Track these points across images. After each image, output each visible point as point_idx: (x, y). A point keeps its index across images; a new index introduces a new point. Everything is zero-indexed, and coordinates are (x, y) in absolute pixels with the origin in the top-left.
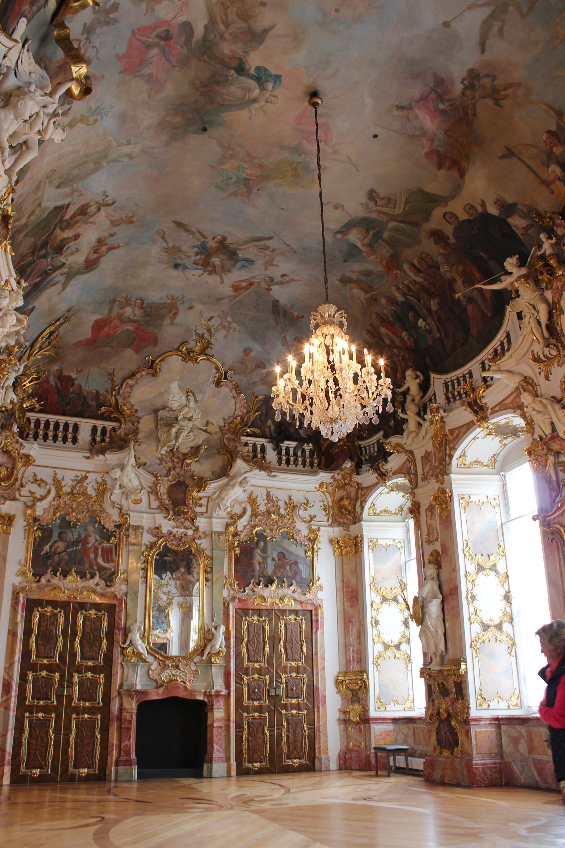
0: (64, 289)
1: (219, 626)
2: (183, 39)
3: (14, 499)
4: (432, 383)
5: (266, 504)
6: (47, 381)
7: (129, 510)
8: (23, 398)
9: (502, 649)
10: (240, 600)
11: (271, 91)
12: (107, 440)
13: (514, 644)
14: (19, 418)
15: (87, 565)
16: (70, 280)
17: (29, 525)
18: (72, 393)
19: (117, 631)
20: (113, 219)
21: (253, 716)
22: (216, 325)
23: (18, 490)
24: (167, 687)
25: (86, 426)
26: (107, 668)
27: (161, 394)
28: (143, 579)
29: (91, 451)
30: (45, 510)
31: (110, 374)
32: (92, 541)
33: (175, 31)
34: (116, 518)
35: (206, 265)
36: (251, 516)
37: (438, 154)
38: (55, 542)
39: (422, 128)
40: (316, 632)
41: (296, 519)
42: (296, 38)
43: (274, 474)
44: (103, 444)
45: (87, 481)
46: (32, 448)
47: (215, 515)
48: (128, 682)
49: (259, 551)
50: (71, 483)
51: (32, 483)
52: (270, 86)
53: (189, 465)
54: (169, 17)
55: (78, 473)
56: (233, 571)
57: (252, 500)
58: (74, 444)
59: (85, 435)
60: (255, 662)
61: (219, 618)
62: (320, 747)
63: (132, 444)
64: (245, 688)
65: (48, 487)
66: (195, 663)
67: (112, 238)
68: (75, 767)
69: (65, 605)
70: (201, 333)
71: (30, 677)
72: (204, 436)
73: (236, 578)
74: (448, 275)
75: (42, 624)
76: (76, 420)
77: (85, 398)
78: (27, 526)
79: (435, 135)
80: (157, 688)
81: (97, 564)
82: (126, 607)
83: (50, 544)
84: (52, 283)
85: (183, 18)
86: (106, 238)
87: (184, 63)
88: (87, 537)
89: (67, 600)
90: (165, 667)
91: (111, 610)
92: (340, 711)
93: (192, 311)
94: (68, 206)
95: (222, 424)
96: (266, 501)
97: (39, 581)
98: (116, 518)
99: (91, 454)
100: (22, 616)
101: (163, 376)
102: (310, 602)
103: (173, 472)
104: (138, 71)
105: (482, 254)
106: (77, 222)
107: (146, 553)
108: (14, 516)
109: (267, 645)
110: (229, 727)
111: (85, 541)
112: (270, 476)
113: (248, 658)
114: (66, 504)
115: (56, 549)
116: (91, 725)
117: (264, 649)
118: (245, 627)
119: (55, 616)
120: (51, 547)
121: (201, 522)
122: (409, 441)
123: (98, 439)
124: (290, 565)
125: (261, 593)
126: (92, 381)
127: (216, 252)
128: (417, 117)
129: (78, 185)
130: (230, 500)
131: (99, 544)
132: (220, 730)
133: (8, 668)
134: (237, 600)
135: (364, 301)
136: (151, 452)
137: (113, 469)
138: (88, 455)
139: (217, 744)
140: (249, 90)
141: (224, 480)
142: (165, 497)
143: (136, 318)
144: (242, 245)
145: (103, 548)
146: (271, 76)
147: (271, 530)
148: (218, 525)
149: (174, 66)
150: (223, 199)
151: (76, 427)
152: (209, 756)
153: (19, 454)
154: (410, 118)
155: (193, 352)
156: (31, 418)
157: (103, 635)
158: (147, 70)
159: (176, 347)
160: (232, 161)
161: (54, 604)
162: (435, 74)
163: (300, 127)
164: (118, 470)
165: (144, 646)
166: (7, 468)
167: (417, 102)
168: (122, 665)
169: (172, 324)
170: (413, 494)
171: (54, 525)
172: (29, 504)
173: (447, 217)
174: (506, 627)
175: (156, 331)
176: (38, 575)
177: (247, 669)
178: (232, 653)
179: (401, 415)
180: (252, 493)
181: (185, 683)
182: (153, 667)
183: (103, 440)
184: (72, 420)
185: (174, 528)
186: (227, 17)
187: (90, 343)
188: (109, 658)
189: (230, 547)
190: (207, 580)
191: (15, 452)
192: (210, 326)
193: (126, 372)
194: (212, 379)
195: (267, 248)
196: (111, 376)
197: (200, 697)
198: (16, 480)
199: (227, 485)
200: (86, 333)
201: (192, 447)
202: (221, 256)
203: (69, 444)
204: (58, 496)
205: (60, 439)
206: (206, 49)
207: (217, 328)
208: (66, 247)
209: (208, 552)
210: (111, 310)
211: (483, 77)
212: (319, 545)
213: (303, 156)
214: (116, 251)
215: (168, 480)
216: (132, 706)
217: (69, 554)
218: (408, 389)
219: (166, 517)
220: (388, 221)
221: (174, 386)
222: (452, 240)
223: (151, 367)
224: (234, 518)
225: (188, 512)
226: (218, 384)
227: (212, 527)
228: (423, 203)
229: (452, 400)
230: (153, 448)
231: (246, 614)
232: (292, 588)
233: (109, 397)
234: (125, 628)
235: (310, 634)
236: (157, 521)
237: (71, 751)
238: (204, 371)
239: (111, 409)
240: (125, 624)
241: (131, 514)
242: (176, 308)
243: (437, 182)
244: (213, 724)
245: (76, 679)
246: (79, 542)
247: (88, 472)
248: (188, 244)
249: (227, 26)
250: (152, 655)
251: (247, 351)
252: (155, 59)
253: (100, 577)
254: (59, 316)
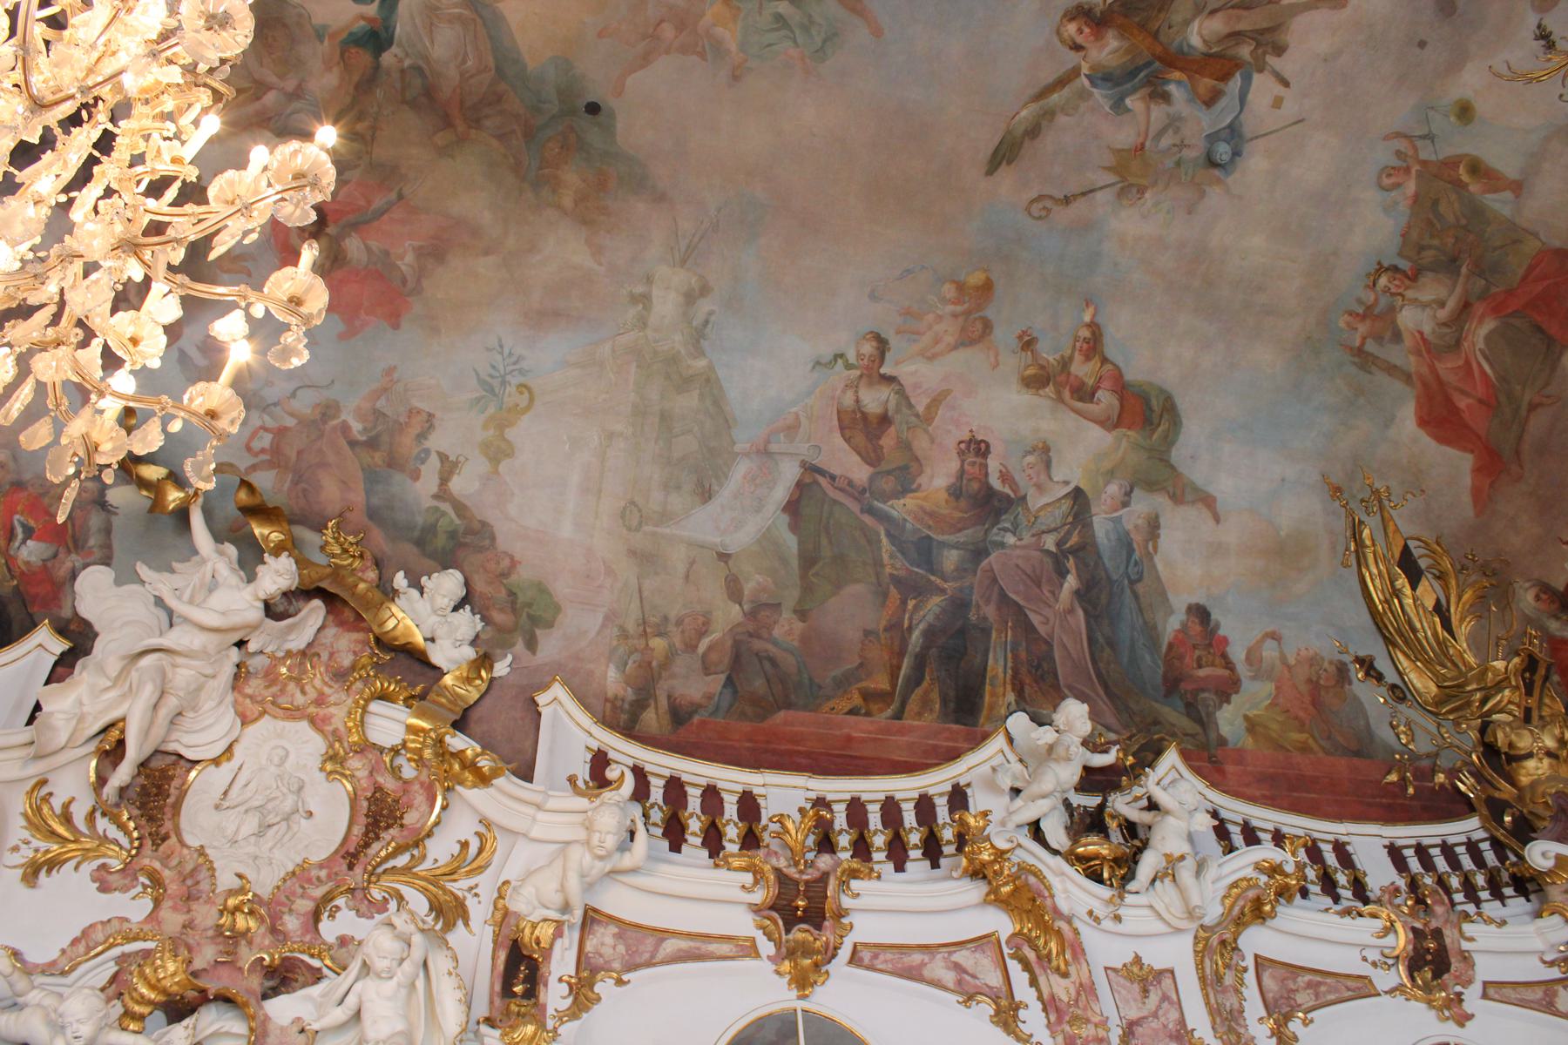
0: (1208, 501)
20: (949, 339)
84: (1137, 538)
104: (404, 282)
106: (905, 446)
127: (1155, 35)
149: (401, 197)
150: (877, 32)
160: (708, 18)
175: (1531, 247)
208: (995, 482)
210: (1391, 369)
252: (374, 244)
254: (1341, 525)
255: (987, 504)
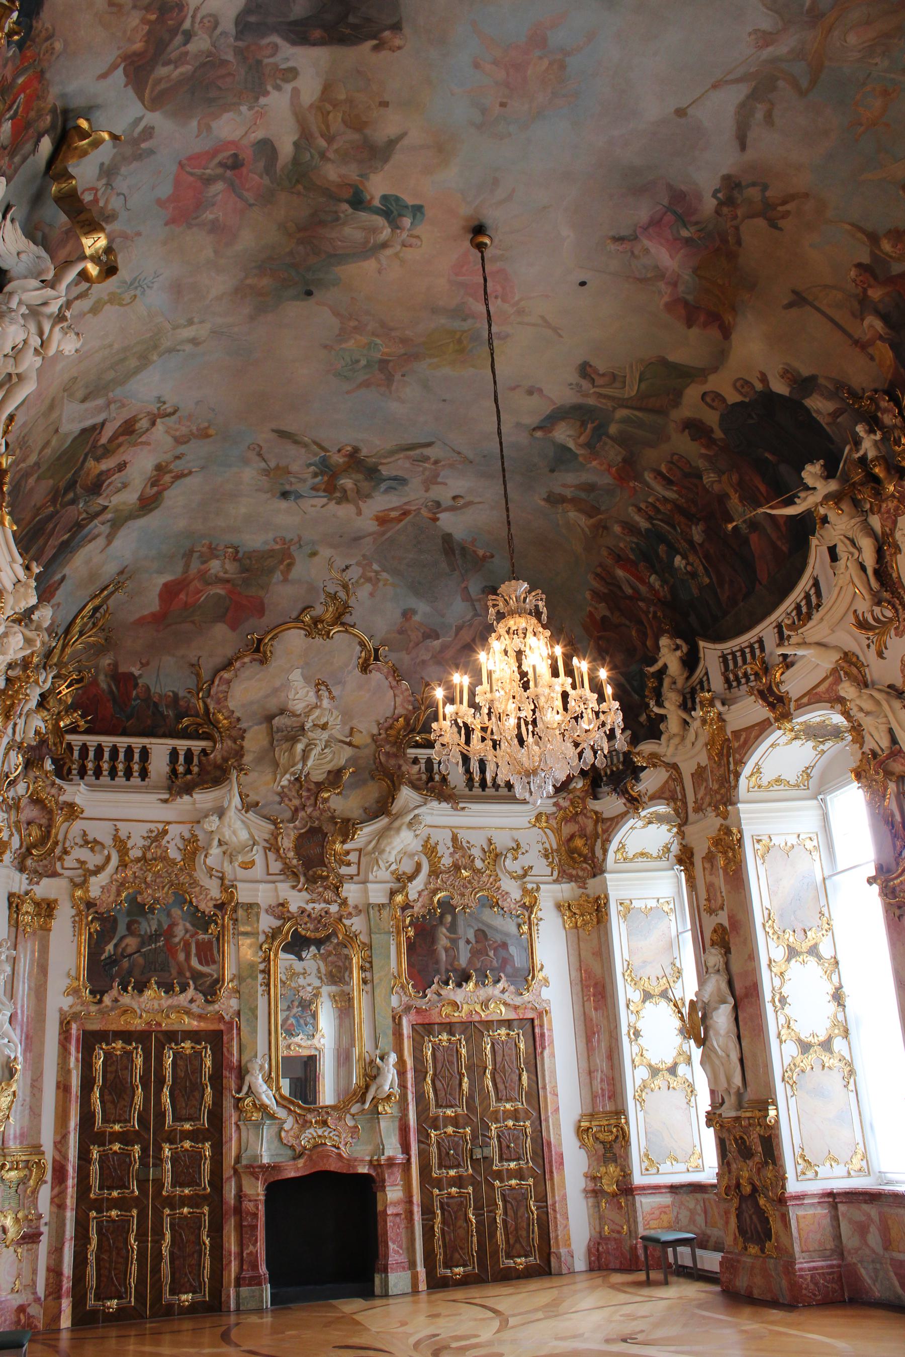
1: (388, 1054)
2: (261, 164)
3: (55, 874)
4: (701, 655)
5: (452, 855)
6: (95, 682)
7: (236, 880)
8: (59, 713)
9: (834, 1081)
10: (419, 1011)
11: (409, 230)
12: (195, 769)
13: (852, 1072)
14: (55, 744)
15: (174, 972)
16: (119, 528)
17: (79, 913)
18: (135, 700)
19: (227, 1073)
20: (178, 434)
21: (449, 1194)
22: (356, 576)
23: (60, 859)
24: (310, 1156)
25: (160, 750)
26: (215, 1133)
27: (276, 691)
28: (264, 988)
29: (170, 789)
30: (103, 887)
31: (193, 665)
32: (179, 931)
33: (247, 154)
34: (215, 892)
35: (331, 489)
36: (430, 876)
37: (686, 303)
38: (122, 938)
39: (657, 267)
40: (542, 1053)
41: (501, 875)
42: (442, 148)
43: (461, 805)
44: (189, 777)
45: (167, 838)
46: (78, 793)
47: (371, 878)
48: (249, 1152)
49: (444, 930)
50: (141, 843)
51: (81, 846)
52: (407, 222)
53: (326, 800)
54: (236, 135)
55: (152, 826)
56: (404, 965)
57: (430, 850)
58: (143, 780)
59: (159, 764)
60: (447, 1107)
61: (387, 1041)
62: (557, 1236)
63: (234, 773)
64: (434, 1150)
65: (106, 852)
66: (353, 1115)
67: (178, 462)
68: (173, 1292)
69: (142, 1037)
70: (332, 592)
71: (95, 1155)
72: (348, 752)
73: (411, 976)
74: (716, 487)
75: (109, 1069)
76: (145, 741)
77: (156, 705)
78: (77, 915)
79: (679, 275)
80: (294, 1159)
81: (191, 968)
82: (239, 1034)
83: (114, 941)
84: (89, 537)
85: (259, 135)
86: (168, 464)
87: (267, 198)
88: (172, 926)
89: (147, 1028)
90: (305, 1125)
91: (216, 1039)
92: (586, 1176)
93: (316, 559)
94: (103, 424)
95: (375, 731)
96: (452, 850)
97: (100, 1001)
98: (215, 892)
99: (171, 794)
100: (77, 1060)
101: (275, 664)
102: (530, 1005)
103: (301, 814)
105: (767, 455)
106: (120, 445)
107: (265, 946)
108: (56, 901)
109: (466, 1079)
110: (410, 1213)
111: (169, 933)
112: (456, 809)
113: (437, 1101)
114: (136, 877)
115: (124, 949)
116: (195, 1224)
117: (460, 1085)
118: (429, 1053)
119: (128, 1055)
120: (116, 946)
121: (350, 891)
122: (671, 749)
123: (181, 769)
124: (495, 950)
125: (452, 996)
126: (165, 678)
127: (345, 471)
128: (647, 251)
129: (118, 393)
130: (394, 853)
131: (192, 936)
132: (398, 1219)
133: (60, 1142)
134: (413, 1011)
135: (586, 529)
136: (264, 784)
137: (206, 816)
138: (166, 796)
139: (394, 1243)
140: (375, 230)
141: (383, 821)
142: (291, 854)
143: (227, 576)
144: (386, 457)
145: (197, 943)
146: (407, 207)
147: (462, 895)
148: (377, 894)
149: (251, 205)
150: (348, 392)
151: (145, 753)
152: (381, 1262)
153: (57, 803)
154: (636, 252)
155: (322, 622)
156: (73, 743)
157: (206, 1080)
158: (209, 216)
159: (293, 616)
160: (358, 337)
161: (126, 1036)
162: (670, 187)
163: (461, 278)
164: (215, 818)
165: (271, 1093)
166: (40, 826)
167: (645, 229)
168: (238, 1126)
169: (285, 580)
170: (681, 834)
171: (119, 910)
172: (78, 880)
173: (708, 399)
174: (839, 1044)
175: (261, 593)
176: (98, 992)
177: (436, 1118)
178: (410, 1097)
179: (656, 710)
180: (429, 838)
181: (338, 1148)
182: (287, 1127)
183: (188, 771)
184: (137, 742)
185: (307, 902)
186: (328, 127)
187: (159, 619)
188: (216, 1116)
189: (397, 927)
190: (365, 982)
191: (50, 801)
192: (347, 579)
193: (218, 660)
194: (354, 661)
195: (426, 459)
196: (195, 667)
197: (363, 1170)
198: (56, 843)
199: (388, 828)
200: (151, 603)
201: (329, 772)
202: (353, 476)
203: (136, 780)
204: (123, 865)
205: (121, 774)
206: (300, 175)
207: (357, 582)
209: (363, 938)
210: (187, 566)
211: (748, 186)
212: (540, 914)
213: (470, 321)
214: (187, 480)
215: (295, 827)
216: (257, 1190)
217: (144, 955)
218: (665, 666)
219: (294, 887)
220: (614, 409)
221: (296, 676)
222: (718, 434)
223: (257, 650)
224: (403, 880)
225: (328, 877)
226: (365, 668)
227: (367, 897)
228: (667, 380)
229: (735, 684)
230: (269, 777)
231: (430, 1033)
232: (500, 986)
233: (194, 700)
234: (240, 1066)
235: (532, 1056)
236: (280, 894)
237: (166, 1267)
238: (342, 649)
239: (199, 720)
240: (240, 1061)
241: (239, 885)
242: (290, 556)
243: (687, 346)
244: (385, 1210)
245: (167, 1153)
246: (160, 935)
247: (168, 823)
248: (299, 461)
249: (330, 139)
250: (284, 1107)
251: (407, 614)
253: (196, 989)
254: (106, 583)
255: (96, 487)
